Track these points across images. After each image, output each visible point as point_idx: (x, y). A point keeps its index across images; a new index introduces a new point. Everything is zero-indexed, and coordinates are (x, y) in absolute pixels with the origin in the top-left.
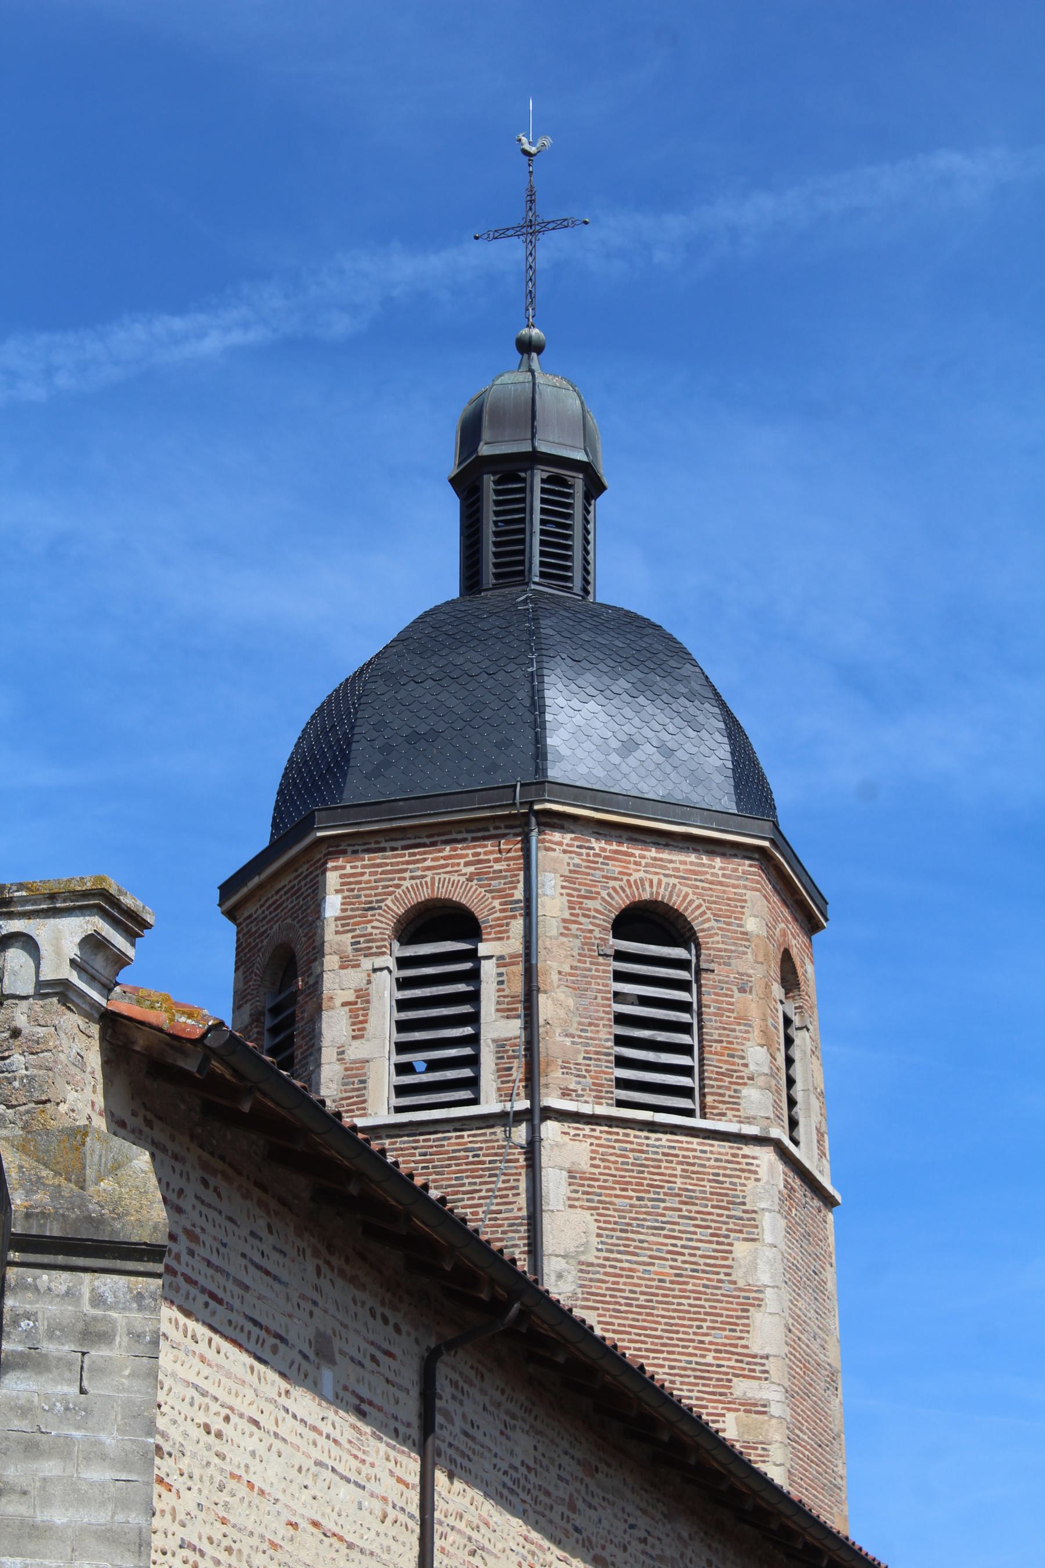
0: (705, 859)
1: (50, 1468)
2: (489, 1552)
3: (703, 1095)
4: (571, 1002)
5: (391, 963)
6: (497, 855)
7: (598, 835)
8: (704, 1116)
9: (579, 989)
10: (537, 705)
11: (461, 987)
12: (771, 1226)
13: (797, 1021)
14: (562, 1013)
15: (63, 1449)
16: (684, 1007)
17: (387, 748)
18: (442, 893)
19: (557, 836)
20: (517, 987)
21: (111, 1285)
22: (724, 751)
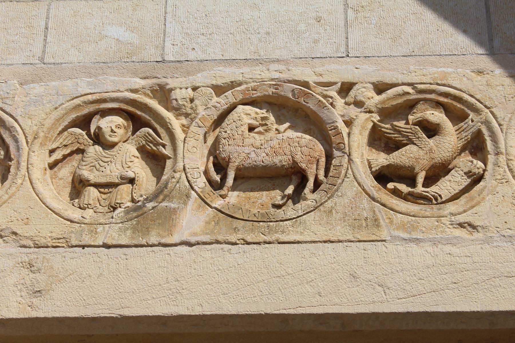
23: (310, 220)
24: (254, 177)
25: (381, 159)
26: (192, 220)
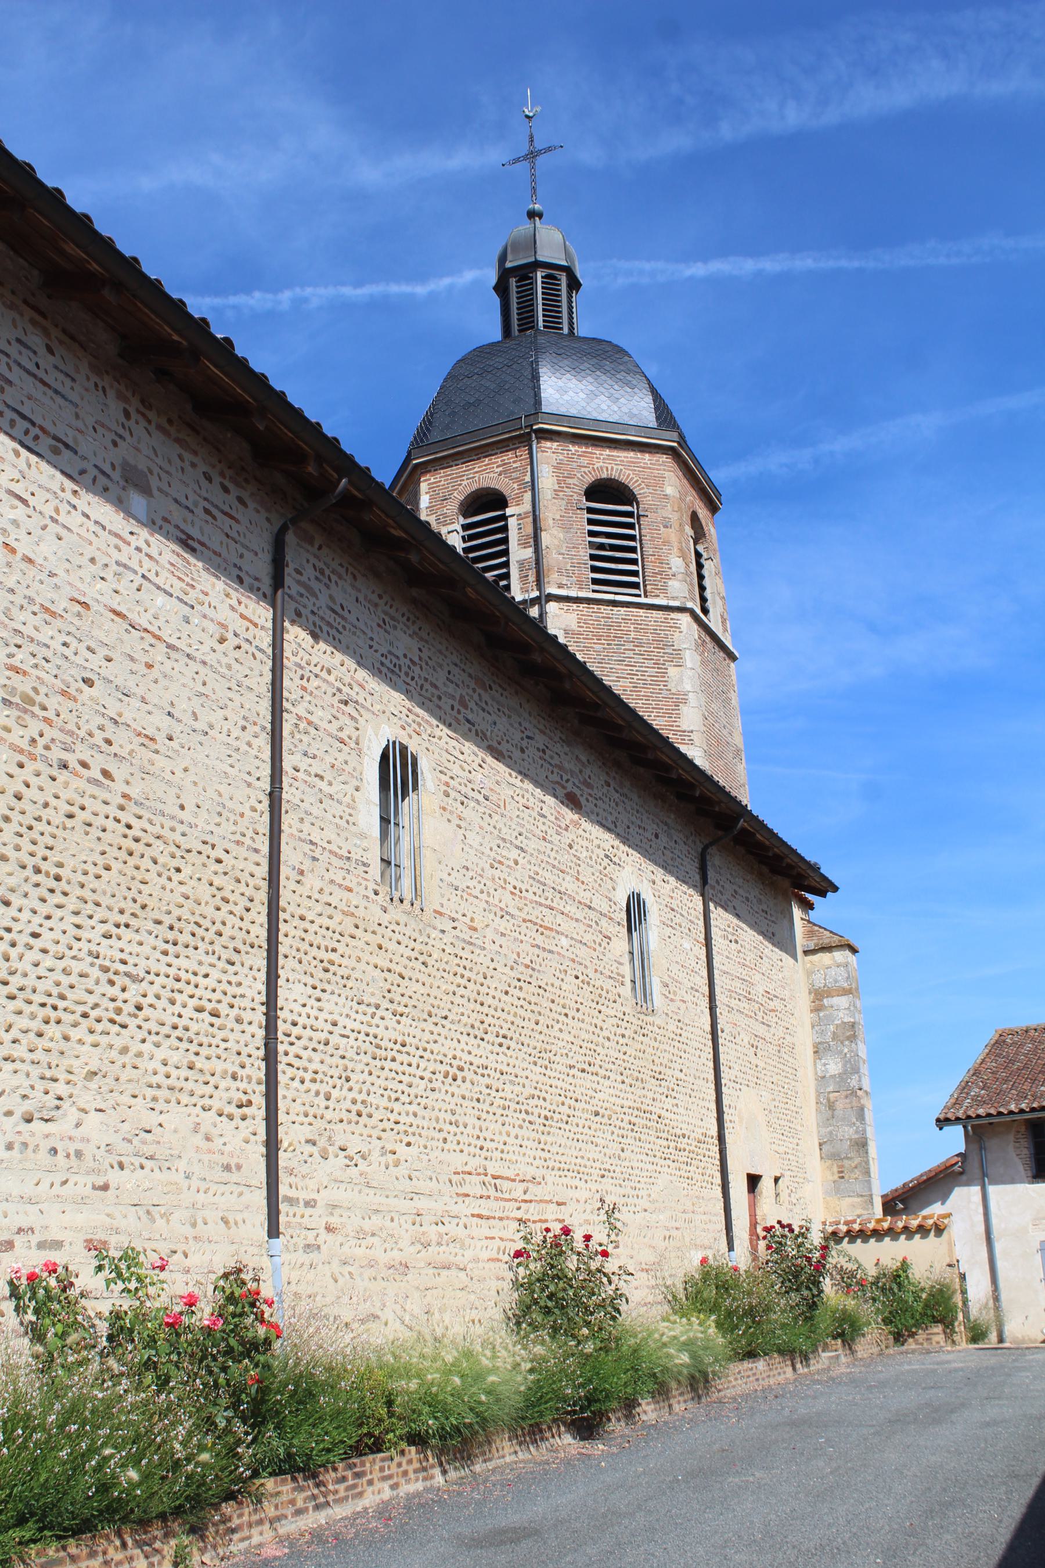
0: (639, 455)
2: (363, 707)
3: (645, 586)
4: (561, 535)
5: (459, 529)
6: (514, 459)
7: (574, 443)
8: (646, 596)
9: (566, 528)
10: (535, 378)
11: (499, 536)
12: (691, 658)
13: (705, 555)
14: (556, 542)
16: (632, 538)
17: (453, 414)
18: (485, 485)
19: (548, 444)
20: (530, 530)
22: (649, 399)
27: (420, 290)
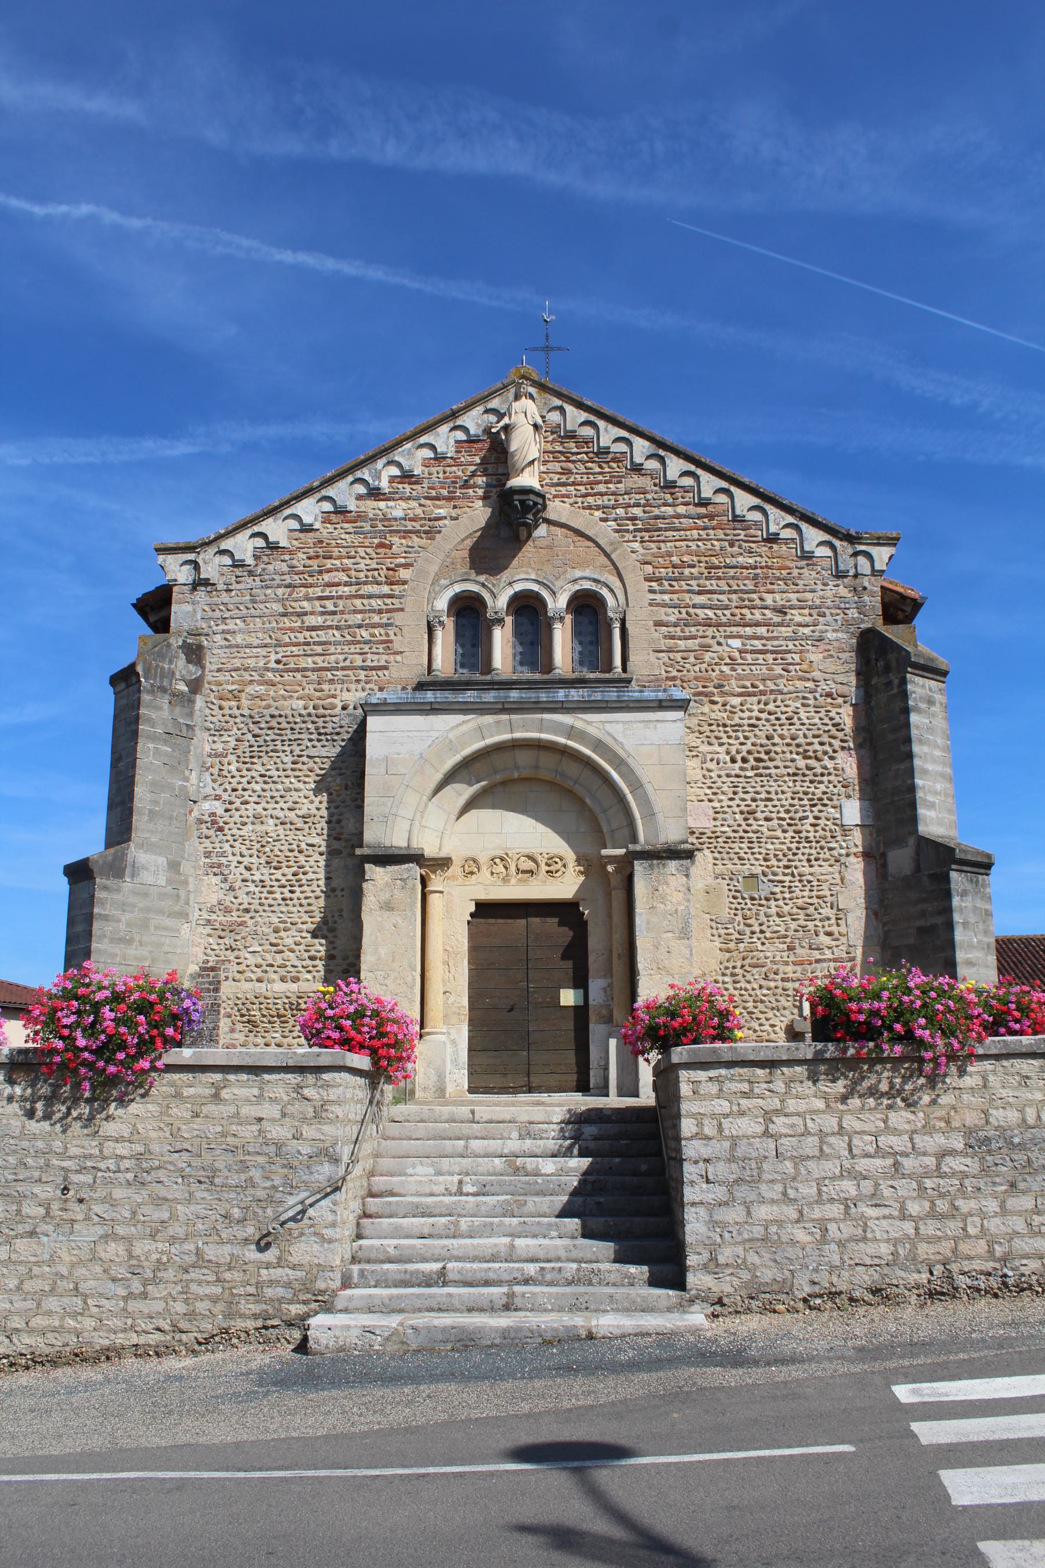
1: (926, 749)
15: (927, 743)
21: (933, 683)
23: (534, 881)
24: (524, 872)
25: (548, 868)
26: (513, 881)
27: (38, 210)
